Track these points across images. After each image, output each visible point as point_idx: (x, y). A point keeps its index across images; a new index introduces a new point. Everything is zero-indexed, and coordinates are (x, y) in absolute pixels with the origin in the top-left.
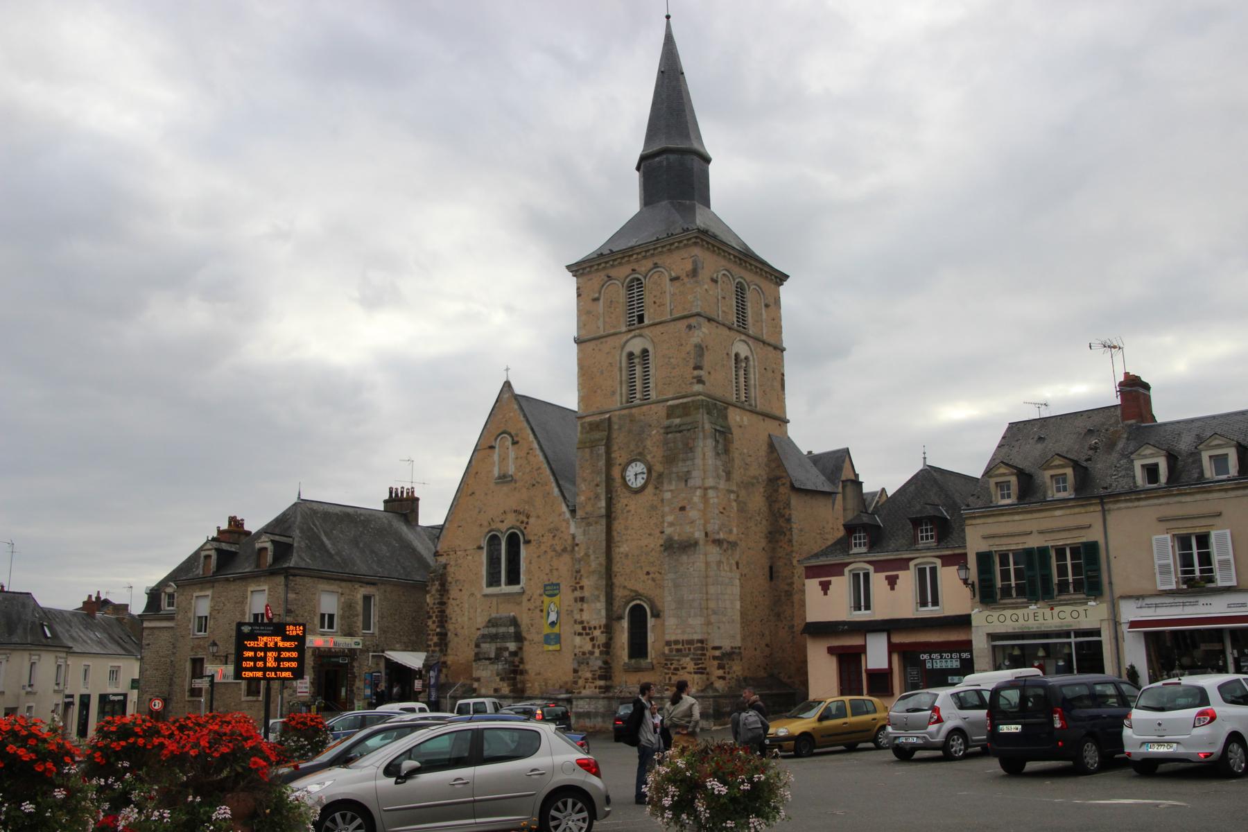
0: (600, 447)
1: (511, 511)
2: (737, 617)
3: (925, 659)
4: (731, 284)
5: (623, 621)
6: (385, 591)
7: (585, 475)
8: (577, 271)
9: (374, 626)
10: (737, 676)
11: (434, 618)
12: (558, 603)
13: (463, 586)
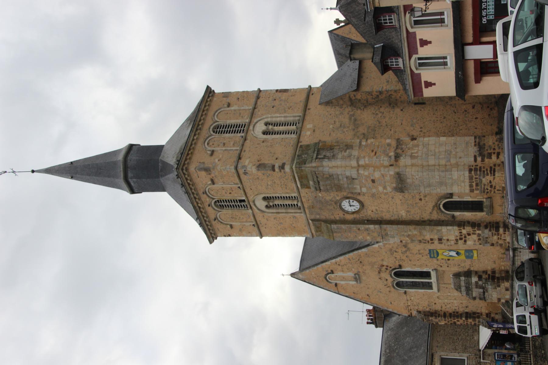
0: (332, 227)
1: (379, 275)
2: (452, 139)
3: (487, 20)
4: (214, 137)
5: (455, 215)
6: (437, 347)
7: (352, 236)
8: (213, 237)
9: (462, 357)
10: (497, 141)
11: (456, 321)
12: (443, 251)
13: (432, 302)
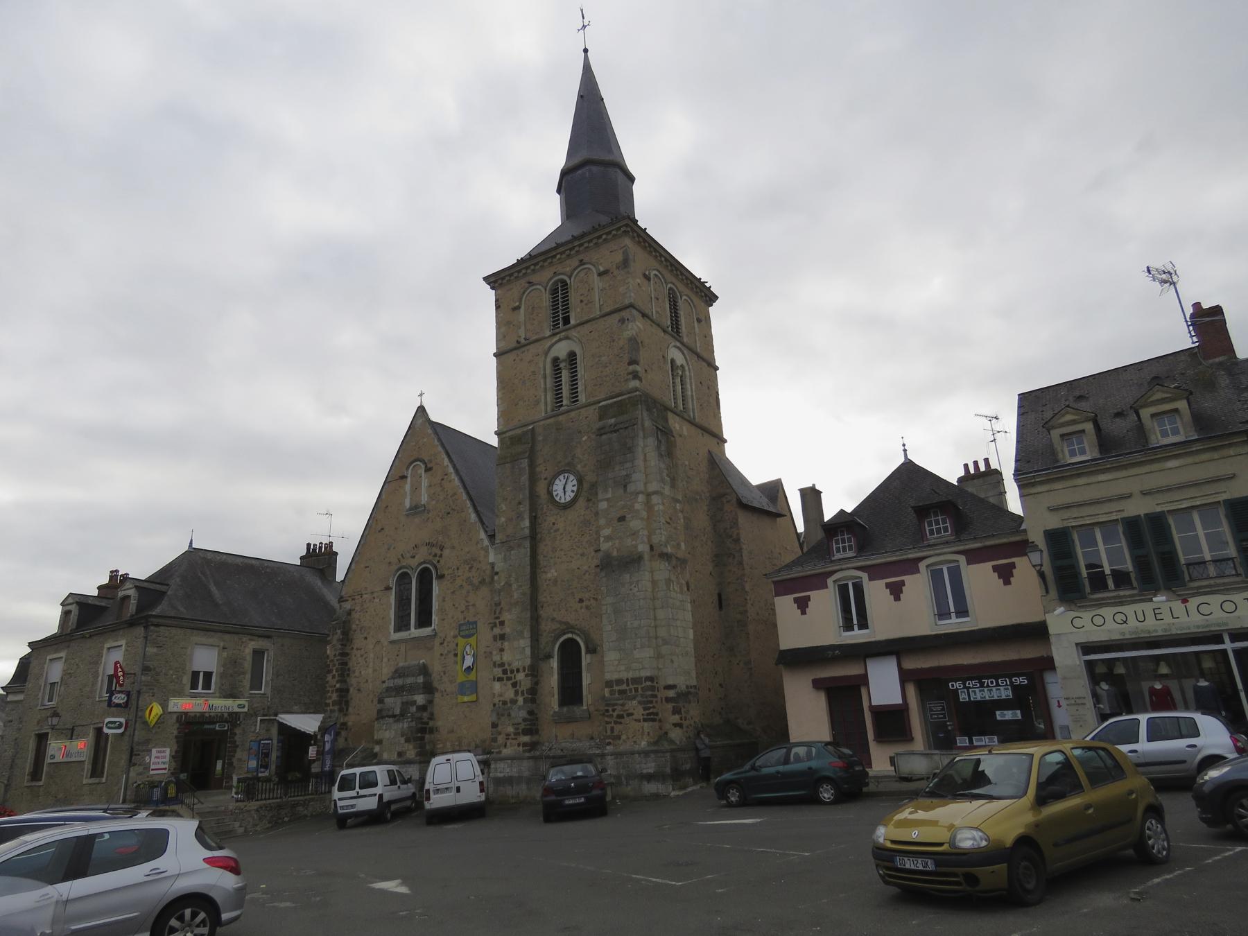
3: (957, 689)
6: (283, 645)
8: (495, 282)
13: (369, 633)
